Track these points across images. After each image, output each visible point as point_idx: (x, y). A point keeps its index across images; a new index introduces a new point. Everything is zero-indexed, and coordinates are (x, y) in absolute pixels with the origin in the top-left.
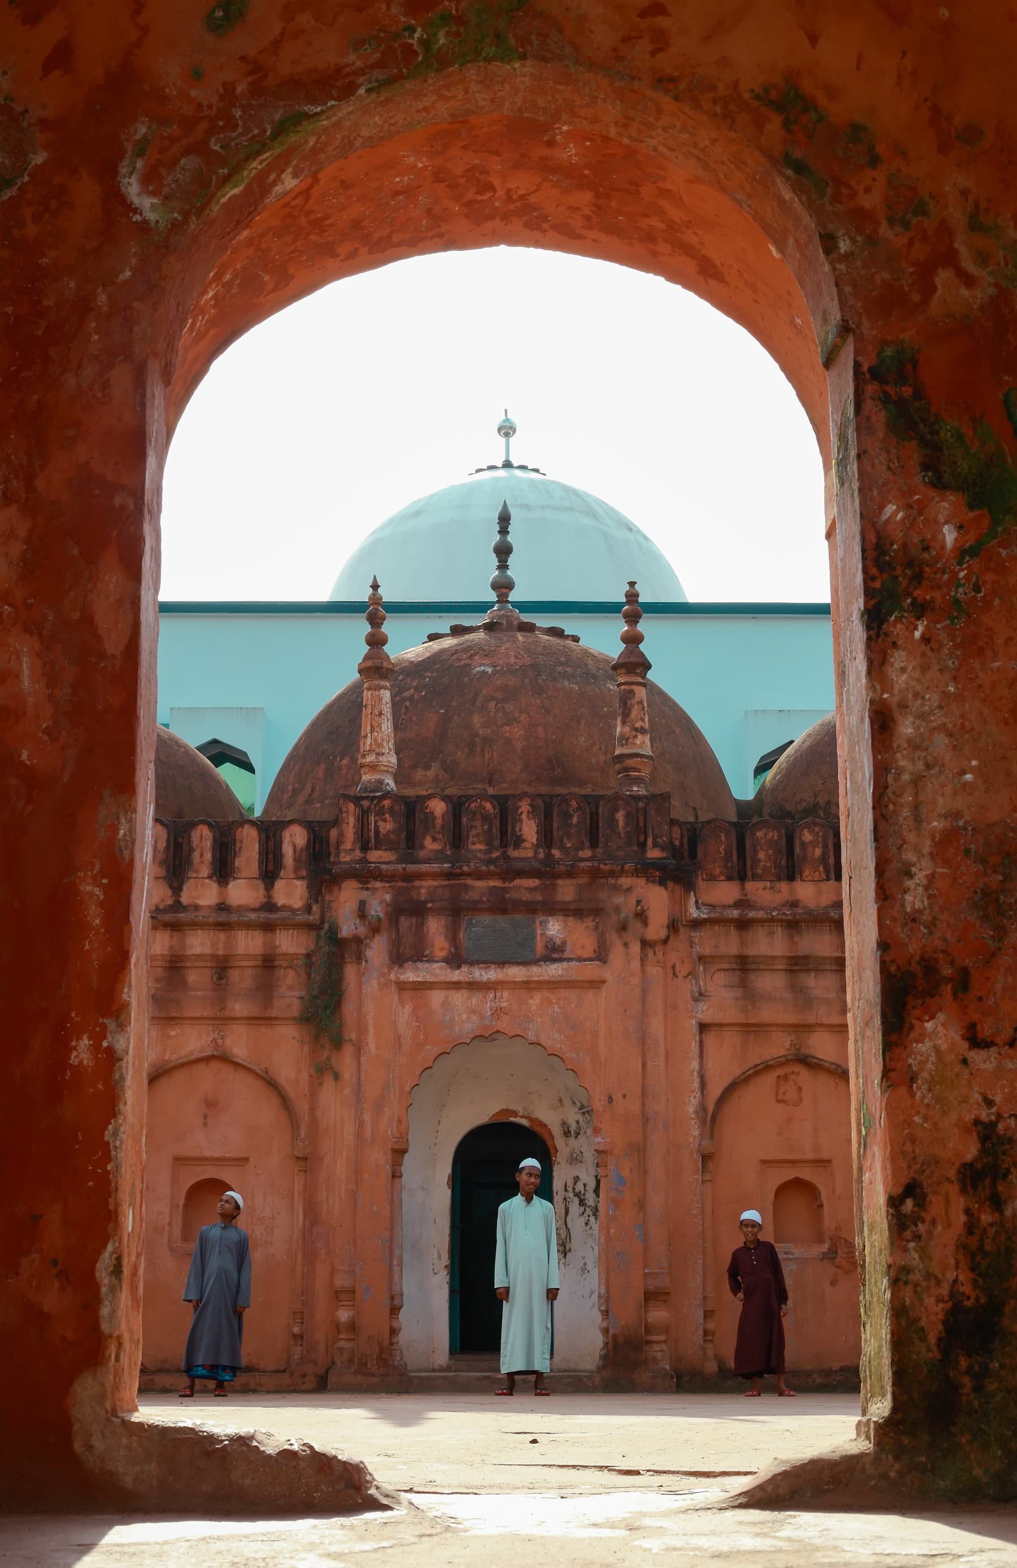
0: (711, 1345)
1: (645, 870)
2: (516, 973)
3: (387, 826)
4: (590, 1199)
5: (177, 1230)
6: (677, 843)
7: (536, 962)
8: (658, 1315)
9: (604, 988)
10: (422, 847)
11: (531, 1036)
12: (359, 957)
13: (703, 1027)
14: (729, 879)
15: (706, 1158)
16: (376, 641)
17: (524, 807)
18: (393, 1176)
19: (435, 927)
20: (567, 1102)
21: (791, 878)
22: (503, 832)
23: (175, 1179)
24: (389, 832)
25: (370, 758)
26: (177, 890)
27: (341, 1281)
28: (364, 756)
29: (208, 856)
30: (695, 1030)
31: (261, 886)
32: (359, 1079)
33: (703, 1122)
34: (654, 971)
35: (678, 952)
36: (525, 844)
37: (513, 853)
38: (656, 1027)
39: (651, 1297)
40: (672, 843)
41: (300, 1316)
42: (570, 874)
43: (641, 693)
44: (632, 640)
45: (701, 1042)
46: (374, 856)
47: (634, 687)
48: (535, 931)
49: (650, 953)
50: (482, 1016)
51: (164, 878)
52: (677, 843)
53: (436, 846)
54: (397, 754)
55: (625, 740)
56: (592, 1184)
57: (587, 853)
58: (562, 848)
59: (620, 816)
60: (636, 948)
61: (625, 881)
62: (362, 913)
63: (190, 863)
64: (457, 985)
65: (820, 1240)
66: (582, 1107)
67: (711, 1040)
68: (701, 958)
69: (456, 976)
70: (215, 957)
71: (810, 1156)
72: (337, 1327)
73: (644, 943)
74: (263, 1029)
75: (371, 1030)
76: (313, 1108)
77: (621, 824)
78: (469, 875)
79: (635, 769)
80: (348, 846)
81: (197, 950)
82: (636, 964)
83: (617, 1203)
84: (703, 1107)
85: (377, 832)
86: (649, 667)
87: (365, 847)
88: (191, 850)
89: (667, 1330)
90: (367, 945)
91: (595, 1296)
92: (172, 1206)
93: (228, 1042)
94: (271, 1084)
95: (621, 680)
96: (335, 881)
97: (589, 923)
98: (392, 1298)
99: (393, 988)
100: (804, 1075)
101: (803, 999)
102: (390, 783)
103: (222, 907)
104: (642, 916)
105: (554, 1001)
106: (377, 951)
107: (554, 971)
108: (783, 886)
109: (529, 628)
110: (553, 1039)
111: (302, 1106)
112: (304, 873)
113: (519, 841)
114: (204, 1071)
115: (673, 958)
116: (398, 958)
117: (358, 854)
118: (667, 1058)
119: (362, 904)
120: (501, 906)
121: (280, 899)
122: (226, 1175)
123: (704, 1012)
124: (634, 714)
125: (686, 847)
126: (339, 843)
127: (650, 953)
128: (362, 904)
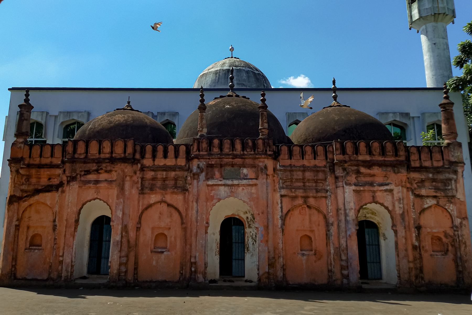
2: (236, 182)
7: (241, 179)
13: (282, 196)
16: (202, 101)
18: (206, 233)
20: (248, 213)
24: (205, 147)
27: (193, 260)
32: (197, 208)
33: (282, 220)
36: (238, 150)
37: (235, 152)
40: (273, 150)
46: (201, 153)
48: (240, 171)
51: (151, 158)
61: (262, 160)
82: (265, 180)
97: (254, 169)
98: (205, 264)
105: (245, 189)
106: (202, 176)
107: (244, 182)
111: (184, 215)
116: (207, 179)
119: (198, 165)
120: (233, 165)
126: (193, 149)
127: (268, 177)
128: (198, 165)
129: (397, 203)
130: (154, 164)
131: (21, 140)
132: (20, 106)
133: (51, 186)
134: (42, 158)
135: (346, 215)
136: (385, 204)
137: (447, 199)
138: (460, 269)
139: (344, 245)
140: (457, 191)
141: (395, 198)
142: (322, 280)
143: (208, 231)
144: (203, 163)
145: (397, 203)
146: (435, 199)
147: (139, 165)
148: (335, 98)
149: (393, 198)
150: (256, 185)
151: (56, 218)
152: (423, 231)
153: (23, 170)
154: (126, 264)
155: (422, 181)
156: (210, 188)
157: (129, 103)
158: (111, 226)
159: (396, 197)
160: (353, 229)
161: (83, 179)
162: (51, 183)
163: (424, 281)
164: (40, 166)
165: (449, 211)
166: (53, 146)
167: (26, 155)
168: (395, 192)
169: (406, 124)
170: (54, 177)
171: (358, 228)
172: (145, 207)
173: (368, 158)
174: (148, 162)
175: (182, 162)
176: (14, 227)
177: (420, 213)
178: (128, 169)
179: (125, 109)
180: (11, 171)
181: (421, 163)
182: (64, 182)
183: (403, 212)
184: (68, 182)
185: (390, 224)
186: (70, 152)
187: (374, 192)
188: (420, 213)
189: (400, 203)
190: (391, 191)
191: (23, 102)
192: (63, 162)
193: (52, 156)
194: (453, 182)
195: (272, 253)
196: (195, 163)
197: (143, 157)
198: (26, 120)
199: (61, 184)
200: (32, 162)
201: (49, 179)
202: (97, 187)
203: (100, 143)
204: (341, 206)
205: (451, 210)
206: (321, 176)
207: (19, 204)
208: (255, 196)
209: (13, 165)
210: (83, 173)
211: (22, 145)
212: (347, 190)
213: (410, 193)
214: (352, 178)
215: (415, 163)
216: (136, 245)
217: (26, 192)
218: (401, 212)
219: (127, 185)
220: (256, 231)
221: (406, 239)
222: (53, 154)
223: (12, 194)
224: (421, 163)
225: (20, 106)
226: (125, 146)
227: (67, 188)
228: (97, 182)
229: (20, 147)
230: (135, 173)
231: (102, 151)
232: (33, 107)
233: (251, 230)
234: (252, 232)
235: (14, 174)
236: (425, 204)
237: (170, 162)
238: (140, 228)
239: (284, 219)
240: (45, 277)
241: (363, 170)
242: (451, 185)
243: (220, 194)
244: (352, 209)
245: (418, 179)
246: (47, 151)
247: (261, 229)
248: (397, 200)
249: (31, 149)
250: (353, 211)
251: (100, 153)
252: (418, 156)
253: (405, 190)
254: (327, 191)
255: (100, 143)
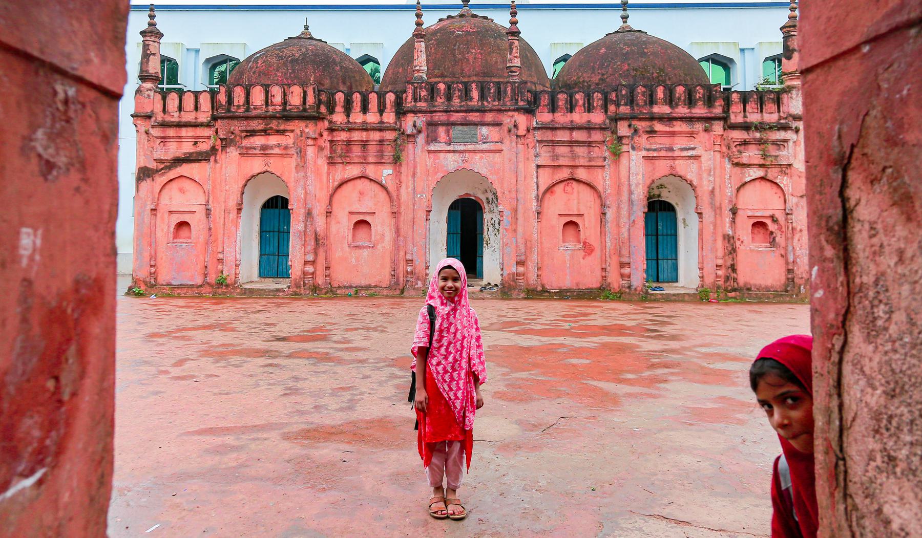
0: (539, 280)
1: (517, 110)
3: (424, 93)
4: (497, 226)
5: (350, 238)
6: (529, 99)
8: (521, 270)
9: (502, 152)
10: (436, 101)
11: (476, 171)
12: (414, 142)
14: (549, 112)
15: (538, 213)
16: (419, 24)
17: (474, 86)
19: (441, 131)
21: (571, 112)
22: (466, 94)
23: (349, 220)
25: (417, 68)
26: (348, 116)
27: (409, 257)
28: (415, 67)
29: (359, 104)
30: (535, 168)
31: (378, 114)
33: (538, 200)
34: (520, 146)
35: (530, 139)
37: (470, 103)
38: (521, 166)
39: (518, 263)
41: (394, 268)
42: (491, 111)
43: (517, 43)
44: (514, 23)
45: (537, 172)
46: (419, 104)
47: (514, 41)
49: (519, 140)
50: (458, 163)
51: (343, 112)
52: (529, 99)
53: (441, 101)
54: (427, 66)
55: (511, 60)
56: (497, 221)
57: (497, 103)
58: (487, 101)
59: (509, 89)
60: (514, 137)
61: (510, 113)
62: (415, 126)
63: (352, 107)
64: (449, 152)
65: (579, 242)
66: (494, 194)
67: (541, 171)
68: (537, 141)
69: (449, 148)
70: (362, 141)
71: (576, 213)
72: (407, 272)
73: (517, 136)
74: (380, 167)
75: (418, 168)
76: (398, 196)
77: (509, 92)
78: (453, 111)
79: (514, 72)
80: (409, 100)
81: (356, 139)
82: (514, 144)
83: (507, 230)
84: (538, 196)
85: (420, 95)
86: (520, 33)
87: (416, 101)
88: (353, 102)
89: (524, 275)
90: (417, 137)
91: (498, 261)
92: (348, 230)
93: (367, 171)
94: (383, 186)
95: (510, 38)
96: (404, 113)
98: (426, 263)
99: (426, 153)
100: (575, 184)
101: (574, 157)
102: (424, 76)
103: (364, 122)
104: (516, 126)
106: (421, 139)
108: (569, 115)
109: (475, 16)
110: (484, 172)
111: (394, 194)
112: (394, 110)
113: (471, 99)
114: (358, 182)
115: (528, 141)
117: (413, 103)
118: (525, 178)
121: (385, 120)
122: (368, 218)
123: (540, 161)
124: (514, 51)
125: (533, 100)
126: (406, 99)
127: (519, 140)
129: (705, 175)
130: (349, 121)
131: (149, 85)
132: (143, 33)
133: (199, 153)
134: (182, 113)
135: (631, 193)
136: (689, 177)
137: (780, 169)
138: (790, 267)
139: (626, 235)
140: (795, 157)
141: (703, 168)
142: (592, 281)
143: (431, 217)
144: (421, 121)
145: (705, 175)
146: (761, 169)
147: (326, 123)
148: (624, 18)
149: (700, 168)
150: (500, 151)
151: (209, 199)
152: (740, 213)
153: (155, 129)
154: (313, 263)
155: (745, 143)
156: (432, 155)
157: (306, 27)
158: (289, 210)
159: (705, 166)
160: (640, 210)
161: (245, 143)
162: (198, 149)
163: (738, 284)
164: (180, 125)
165: (782, 186)
166: (197, 94)
167: (158, 107)
168: (703, 159)
169: (731, 60)
170: (202, 140)
171: (646, 210)
172: (336, 183)
173: (666, 109)
174: (339, 118)
175: (389, 117)
176: (149, 212)
177: (738, 190)
178: (310, 129)
179: (301, 38)
180: (137, 131)
181: (745, 116)
182: (217, 147)
183: (713, 188)
184: (224, 147)
185: (695, 206)
186: (224, 103)
187: (673, 158)
188: (738, 190)
189: (709, 175)
190: (696, 157)
191: (145, 27)
192: (215, 118)
193: (197, 108)
194: (791, 144)
195: (522, 248)
196: (410, 120)
197: (331, 110)
198: (154, 54)
199: (214, 150)
200: (168, 119)
201: (195, 143)
202: (266, 154)
203: (267, 88)
204: (624, 180)
205: (785, 185)
206: (597, 136)
207: (153, 180)
208: (498, 166)
209: (139, 122)
210: (244, 134)
211: (152, 93)
212: (634, 157)
213: (727, 160)
214: (643, 140)
215: (736, 116)
216: (326, 237)
217: (161, 161)
218: (710, 188)
219: (311, 152)
220: (499, 217)
221: (715, 226)
222: (199, 106)
223: (142, 165)
224: (745, 116)
225: (143, 33)
226: (305, 93)
227: (221, 156)
228: (264, 148)
229: (149, 96)
230: (321, 135)
231: (270, 101)
232: (163, 35)
233: (491, 215)
234: (494, 219)
235: (144, 136)
236: (747, 176)
237: (372, 117)
238: (331, 212)
239: (540, 200)
240: (199, 280)
241: (658, 127)
242: (788, 149)
243: (447, 164)
244: (640, 184)
245: (740, 140)
246: (189, 101)
247: (507, 213)
248: (705, 170)
249: (164, 99)
250: (641, 186)
251: (267, 104)
252: (742, 107)
253: (718, 155)
254: (605, 158)
255: (267, 88)
